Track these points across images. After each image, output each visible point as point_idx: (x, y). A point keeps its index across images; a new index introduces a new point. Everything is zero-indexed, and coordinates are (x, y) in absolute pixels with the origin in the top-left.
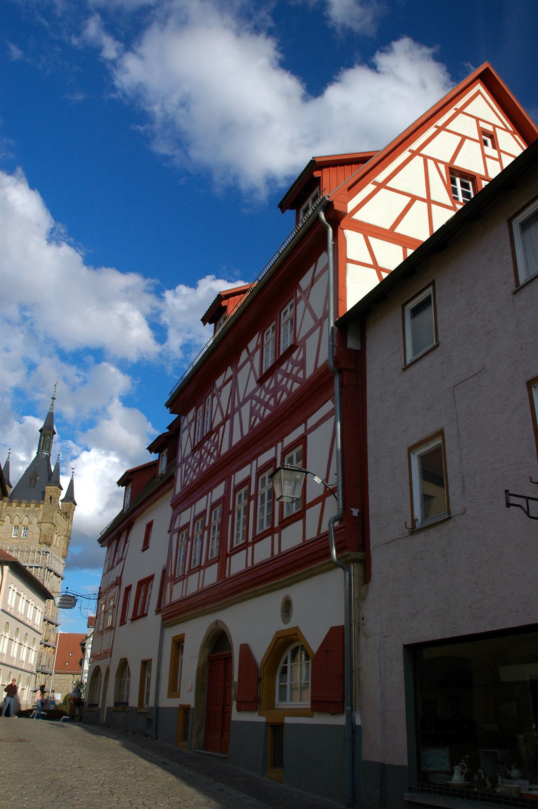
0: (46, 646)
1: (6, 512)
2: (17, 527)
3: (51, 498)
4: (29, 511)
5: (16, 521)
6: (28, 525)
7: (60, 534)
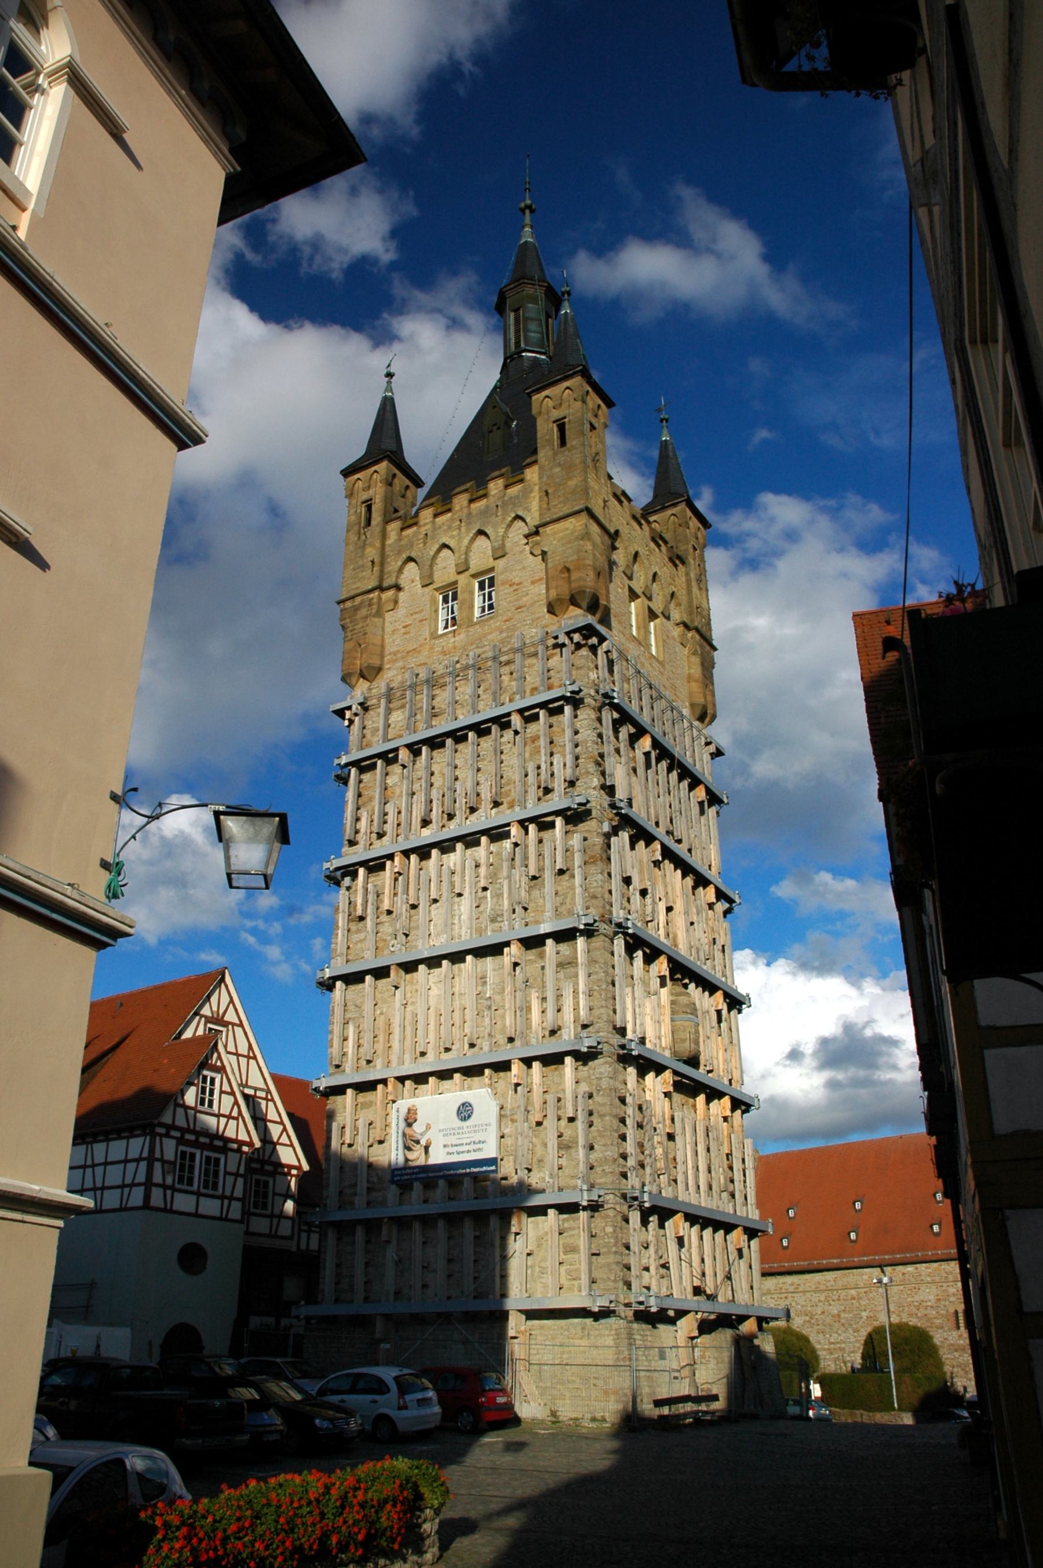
0: (687, 1087)
1: (399, 553)
2: (450, 593)
3: (562, 428)
4: (485, 512)
5: (446, 568)
6: (491, 562)
7: (657, 606)
